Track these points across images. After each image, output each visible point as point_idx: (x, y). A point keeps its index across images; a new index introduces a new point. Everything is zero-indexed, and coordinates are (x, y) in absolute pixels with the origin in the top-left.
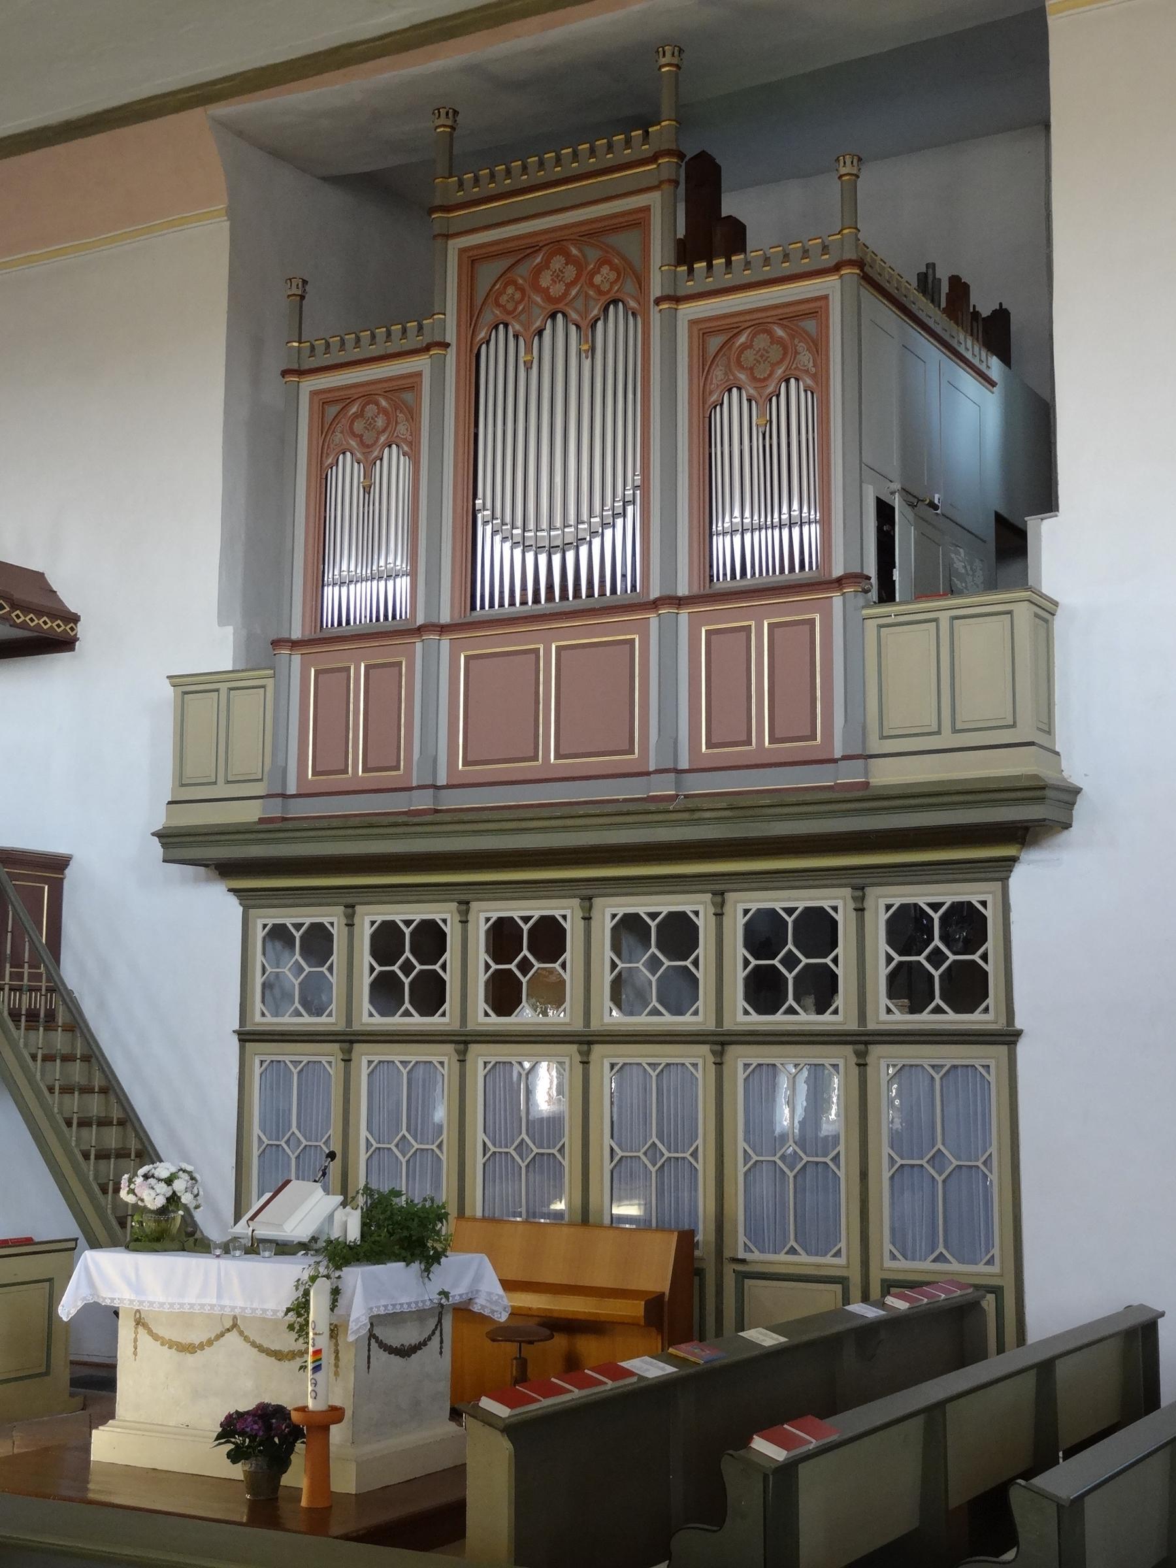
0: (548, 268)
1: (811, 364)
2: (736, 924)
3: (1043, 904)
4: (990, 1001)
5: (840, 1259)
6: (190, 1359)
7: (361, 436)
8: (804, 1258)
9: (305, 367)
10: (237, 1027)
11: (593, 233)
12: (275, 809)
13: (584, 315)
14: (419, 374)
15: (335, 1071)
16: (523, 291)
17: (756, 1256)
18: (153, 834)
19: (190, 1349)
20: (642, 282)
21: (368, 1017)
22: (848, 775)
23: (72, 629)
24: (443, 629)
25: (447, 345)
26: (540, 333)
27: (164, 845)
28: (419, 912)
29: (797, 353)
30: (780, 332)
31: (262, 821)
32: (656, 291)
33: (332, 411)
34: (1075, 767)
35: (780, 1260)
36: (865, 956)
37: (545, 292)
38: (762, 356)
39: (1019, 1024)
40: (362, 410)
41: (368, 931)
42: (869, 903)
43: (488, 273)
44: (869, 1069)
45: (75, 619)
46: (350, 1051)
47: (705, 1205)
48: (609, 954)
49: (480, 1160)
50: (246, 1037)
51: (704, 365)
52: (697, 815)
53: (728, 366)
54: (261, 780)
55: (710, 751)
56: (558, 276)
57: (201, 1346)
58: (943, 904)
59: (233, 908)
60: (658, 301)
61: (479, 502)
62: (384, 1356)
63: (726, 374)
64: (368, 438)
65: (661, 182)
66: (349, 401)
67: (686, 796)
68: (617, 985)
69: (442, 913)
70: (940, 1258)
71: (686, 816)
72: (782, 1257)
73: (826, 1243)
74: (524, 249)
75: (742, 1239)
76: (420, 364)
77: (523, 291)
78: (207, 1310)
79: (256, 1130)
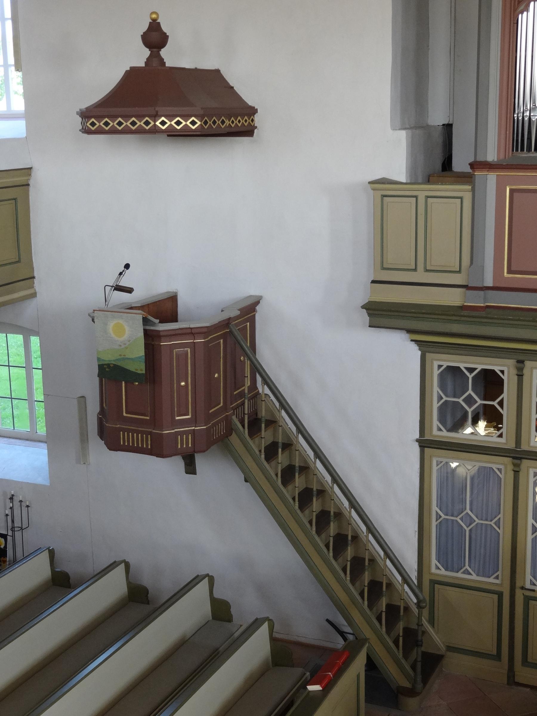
10: (417, 436)
12: (476, 300)
15: (507, 477)
18: (363, 307)
23: (253, 120)
27: (369, 315)
31: (463, 308)
45: (252, 111)
46: (518, 466)
50: (425, 444)
54: (459, 272)
59: (415, 352)
79: (435, 508)
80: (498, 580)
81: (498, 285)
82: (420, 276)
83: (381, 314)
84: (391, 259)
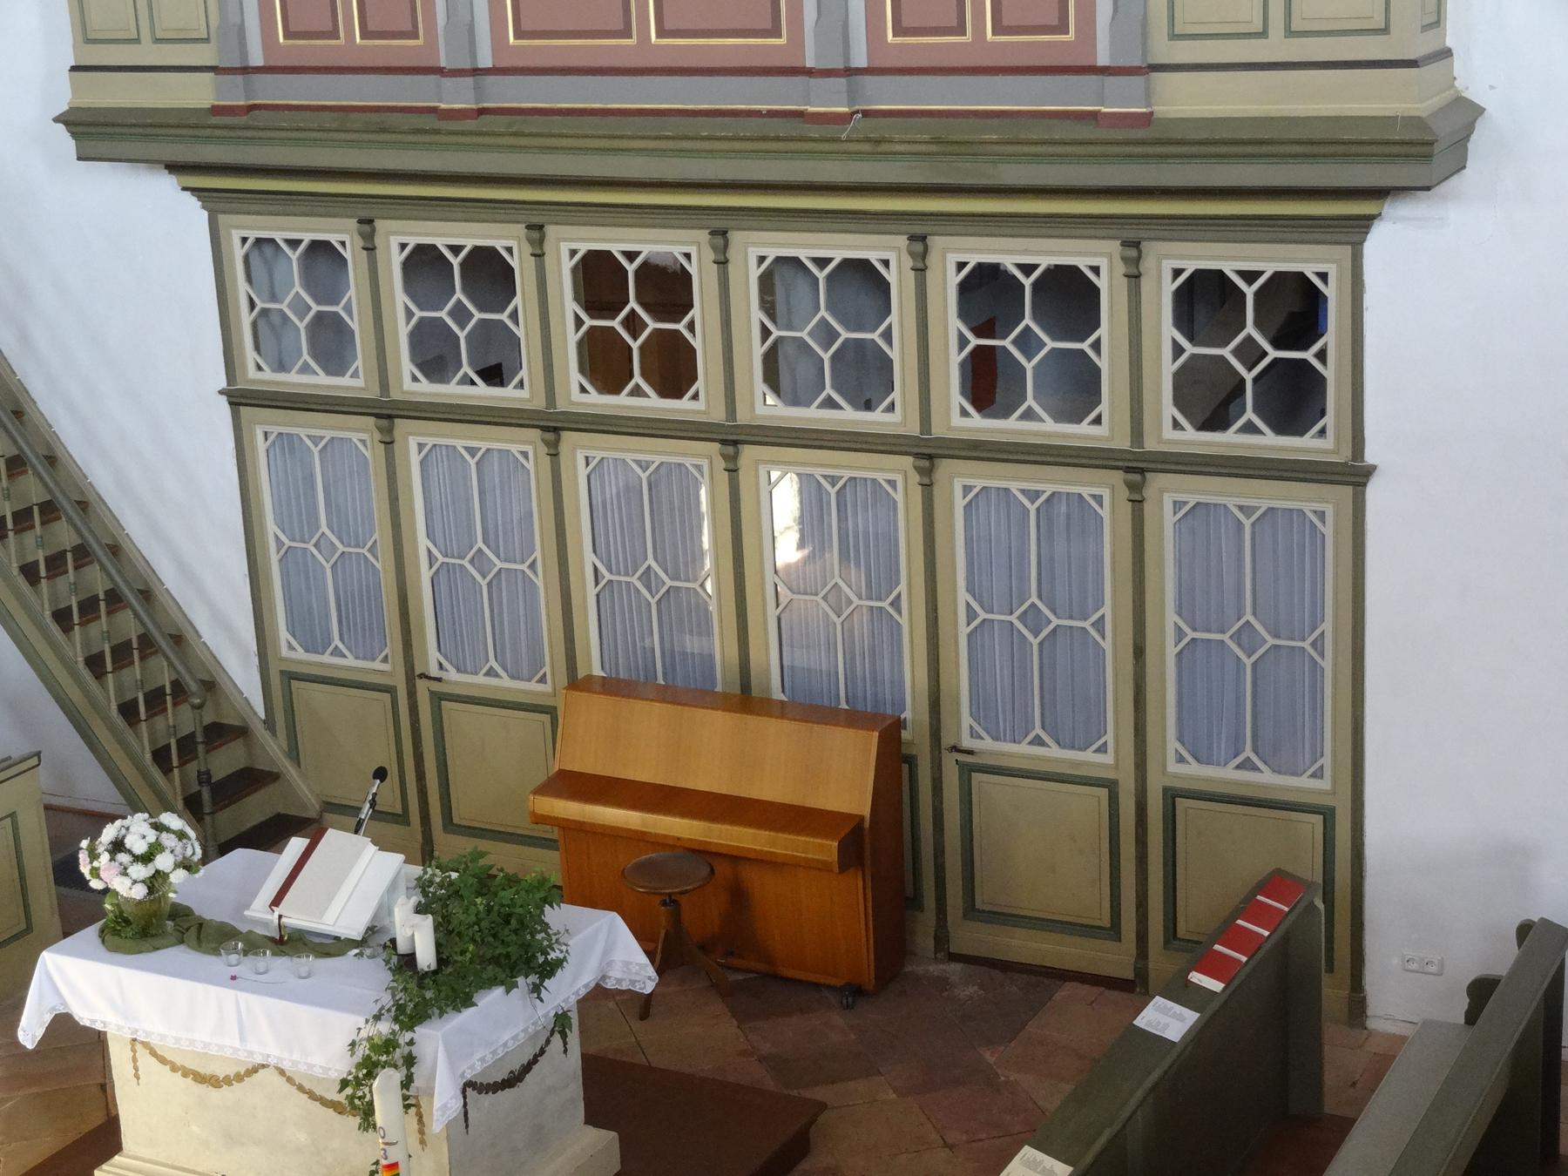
2: (946, 284)
3: (1412, 284)
4: (1329, 420)
5: (1106, 756)
6: (214, 1095)
8: (1054, 752)
10: (223, 384)
12: (235, 94)
15: (372, 453)
17: (987, 744)
18: (56, 120)
19: (214, 1082)
21: (411, 384)
22: (1119, 99)
27: (74, 135)
28: (472, 235)
31: (216, 110)
34: (1474, 75)
35: (1020, 751)
36: (1139, 339)
39: (1370, 457)
41: (397, 259)
42: (1148, 265)
44: (1147, 506)
46: (390, 430)
47: (913, 675)
48: (757, 315)
49: (592, 592)
50: (240, 399)
52: (884, 147)
54: (207, 40)
55: (899, 40)
57: (228, 1081)
58: (1260, 273)
59: (195, 214)
62: (487, 1100)
67: (866, 114)
68: (770, 359)
69: (505, 238)
70: (1247, 765)
71: (866, 147)
72: (1023, 748)
73: (1086, 736)
75: (967, 721)
78: (228, 1053)
79: (271, 527)
80: (383, 666)
81: (272, 63)
82: (147, 54)
83: (97, 133)
84: (99, 22)
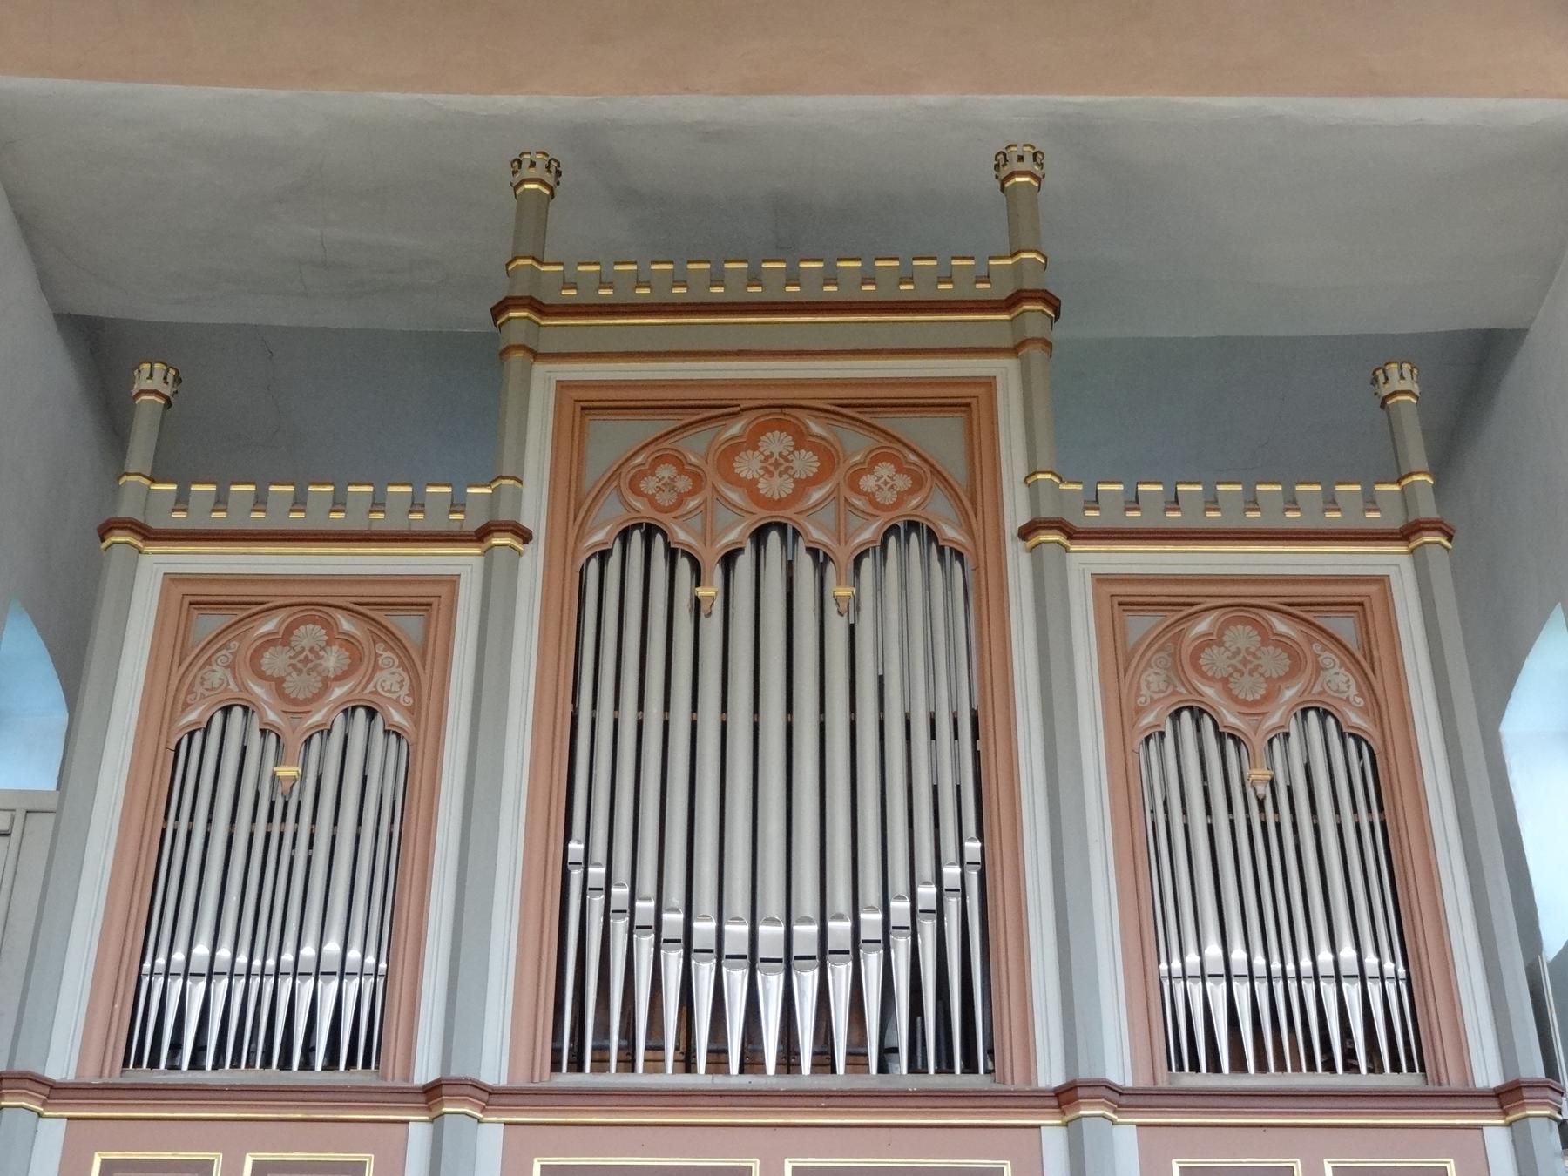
0: (755, 448)
1: (1353, 690)
7: (279, 682)
9: (155, 523)
11: (855, 408)
13: (841, 535)
14: (452, 582)
16: (698, 478)
20: (976, 498)
24: (491, 1097)
25: (525, 536)
26: (729, 560)
29: (1319, 668)
30: (1281, 626)
32: (1017, 512)
33: (213, 622)
37: (750, 487)
38: (1245, 662)
40: (289, 631)
43: (613, 440)
51: (1119, 664)
53: (1176, 668)
56: (777, 465)
60: (1026, 533)
61: (576, 847)
63: (1168, 682)
64: (294, 684)
65: (1023, 343)
66: (262, 609)
74: (710, 409)
76: (463, 561)
77: (698, 478)
